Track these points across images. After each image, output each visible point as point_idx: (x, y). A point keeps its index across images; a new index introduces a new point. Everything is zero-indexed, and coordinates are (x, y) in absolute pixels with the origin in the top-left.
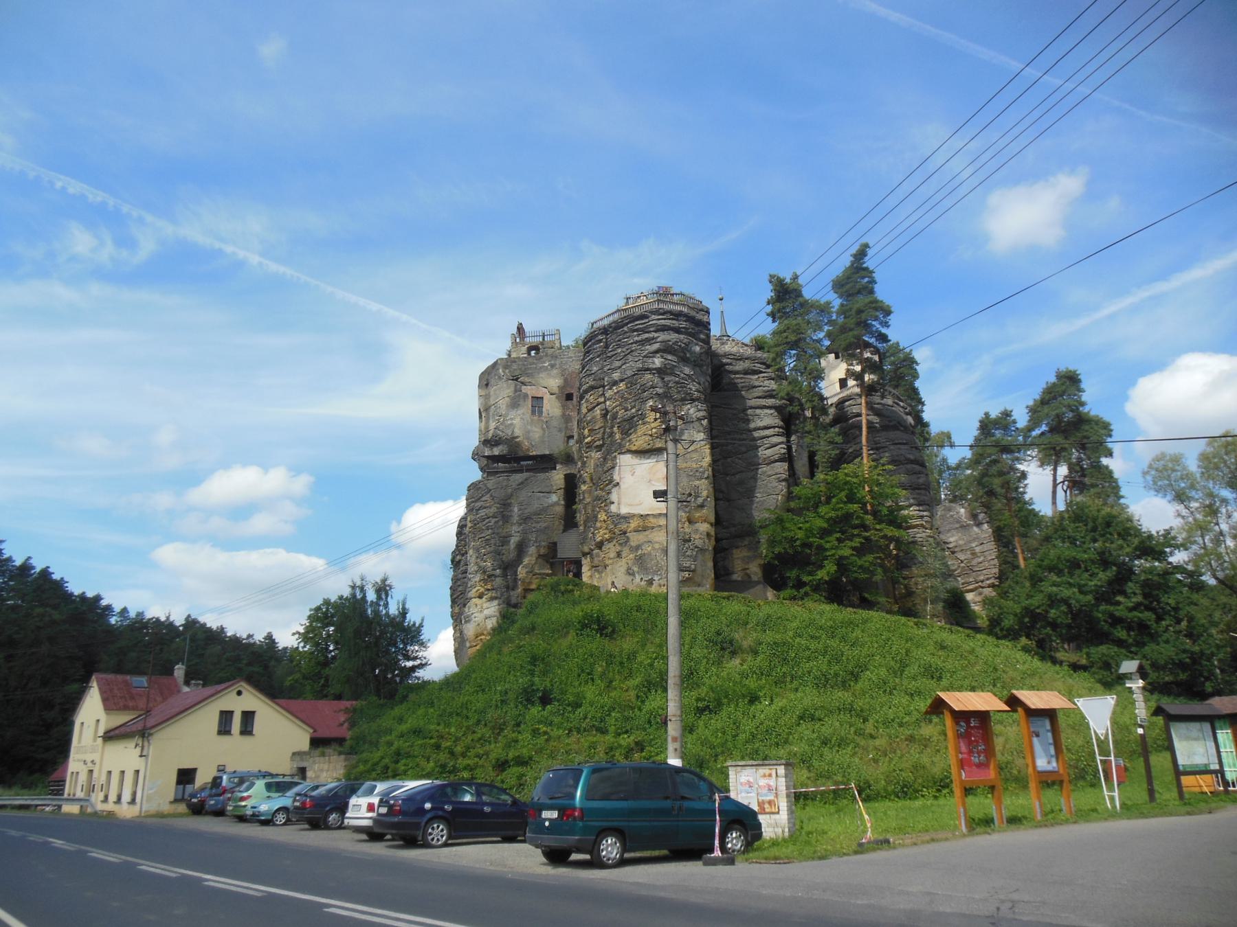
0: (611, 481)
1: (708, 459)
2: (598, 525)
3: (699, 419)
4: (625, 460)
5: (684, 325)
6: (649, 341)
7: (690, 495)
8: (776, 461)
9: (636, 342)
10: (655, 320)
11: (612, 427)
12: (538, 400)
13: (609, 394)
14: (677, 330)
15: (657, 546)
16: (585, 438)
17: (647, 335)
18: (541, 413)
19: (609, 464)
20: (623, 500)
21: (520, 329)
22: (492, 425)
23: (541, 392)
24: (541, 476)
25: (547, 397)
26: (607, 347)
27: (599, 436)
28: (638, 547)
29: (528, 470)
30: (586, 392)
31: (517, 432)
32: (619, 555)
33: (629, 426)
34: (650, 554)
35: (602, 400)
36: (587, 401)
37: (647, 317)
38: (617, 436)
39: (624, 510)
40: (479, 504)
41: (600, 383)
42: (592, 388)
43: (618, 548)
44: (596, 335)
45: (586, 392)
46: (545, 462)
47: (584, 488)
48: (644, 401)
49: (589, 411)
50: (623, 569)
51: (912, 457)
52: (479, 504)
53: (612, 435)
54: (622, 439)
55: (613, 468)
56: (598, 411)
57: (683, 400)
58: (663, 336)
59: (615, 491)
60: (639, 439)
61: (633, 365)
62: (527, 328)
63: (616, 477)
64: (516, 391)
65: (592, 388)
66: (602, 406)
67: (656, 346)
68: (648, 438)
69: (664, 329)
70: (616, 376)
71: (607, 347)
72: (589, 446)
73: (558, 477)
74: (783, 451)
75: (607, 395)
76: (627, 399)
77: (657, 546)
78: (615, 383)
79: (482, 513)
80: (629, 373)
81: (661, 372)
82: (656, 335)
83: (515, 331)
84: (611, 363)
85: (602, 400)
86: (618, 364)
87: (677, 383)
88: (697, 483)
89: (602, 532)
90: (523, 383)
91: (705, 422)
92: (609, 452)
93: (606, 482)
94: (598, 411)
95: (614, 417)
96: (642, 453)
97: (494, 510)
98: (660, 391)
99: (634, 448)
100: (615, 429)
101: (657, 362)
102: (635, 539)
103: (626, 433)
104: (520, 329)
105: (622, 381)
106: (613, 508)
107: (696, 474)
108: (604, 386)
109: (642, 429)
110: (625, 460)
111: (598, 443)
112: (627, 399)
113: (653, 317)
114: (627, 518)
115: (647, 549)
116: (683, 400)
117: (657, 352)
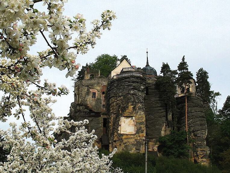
0: (119, 124)
1: (144, 120)
2: (115, 136)
4: (123, 119)
8: (163, 117)
12: (94, 94)
13: (118, 99)
14: (138, 83)
17: (129, 84)
18: (95, 97)
23: (95, 91)
25: (97, 92)
28: (125, 143)
29: (93, 117)
32: (120, 145)
33: (124, 109)
37: (130, 78)
39: (122, 133)
42: (113, 97)
43: (120, 143)
44: (115, 81)
45: (112, 97)
47: (110, 124)
48: (128, 103)
49: (112, 103)
50: (122, 149)
51: (201, 115)
53: (119, 111)
54: (122, 113)
58: (134, 85)
60: (126, 113)
61: (126, 92)
63: (120, 123)
64: (88, 90)
67: (132, 87)
69: (133, 82)
74: (165, 114)
78: (120, 96)
80: (124, 94)
81: (132, 94)
87: (137, 98)
93: (117, 124)
95: (120, 106)
96: (127, 117)
99: (125, 116)
101: (132, 92)
102: (125, 141)
106: (119, 132)
107: (141, 123)
109: (127, 111)
110: (123, 119)
114: (123, 135)
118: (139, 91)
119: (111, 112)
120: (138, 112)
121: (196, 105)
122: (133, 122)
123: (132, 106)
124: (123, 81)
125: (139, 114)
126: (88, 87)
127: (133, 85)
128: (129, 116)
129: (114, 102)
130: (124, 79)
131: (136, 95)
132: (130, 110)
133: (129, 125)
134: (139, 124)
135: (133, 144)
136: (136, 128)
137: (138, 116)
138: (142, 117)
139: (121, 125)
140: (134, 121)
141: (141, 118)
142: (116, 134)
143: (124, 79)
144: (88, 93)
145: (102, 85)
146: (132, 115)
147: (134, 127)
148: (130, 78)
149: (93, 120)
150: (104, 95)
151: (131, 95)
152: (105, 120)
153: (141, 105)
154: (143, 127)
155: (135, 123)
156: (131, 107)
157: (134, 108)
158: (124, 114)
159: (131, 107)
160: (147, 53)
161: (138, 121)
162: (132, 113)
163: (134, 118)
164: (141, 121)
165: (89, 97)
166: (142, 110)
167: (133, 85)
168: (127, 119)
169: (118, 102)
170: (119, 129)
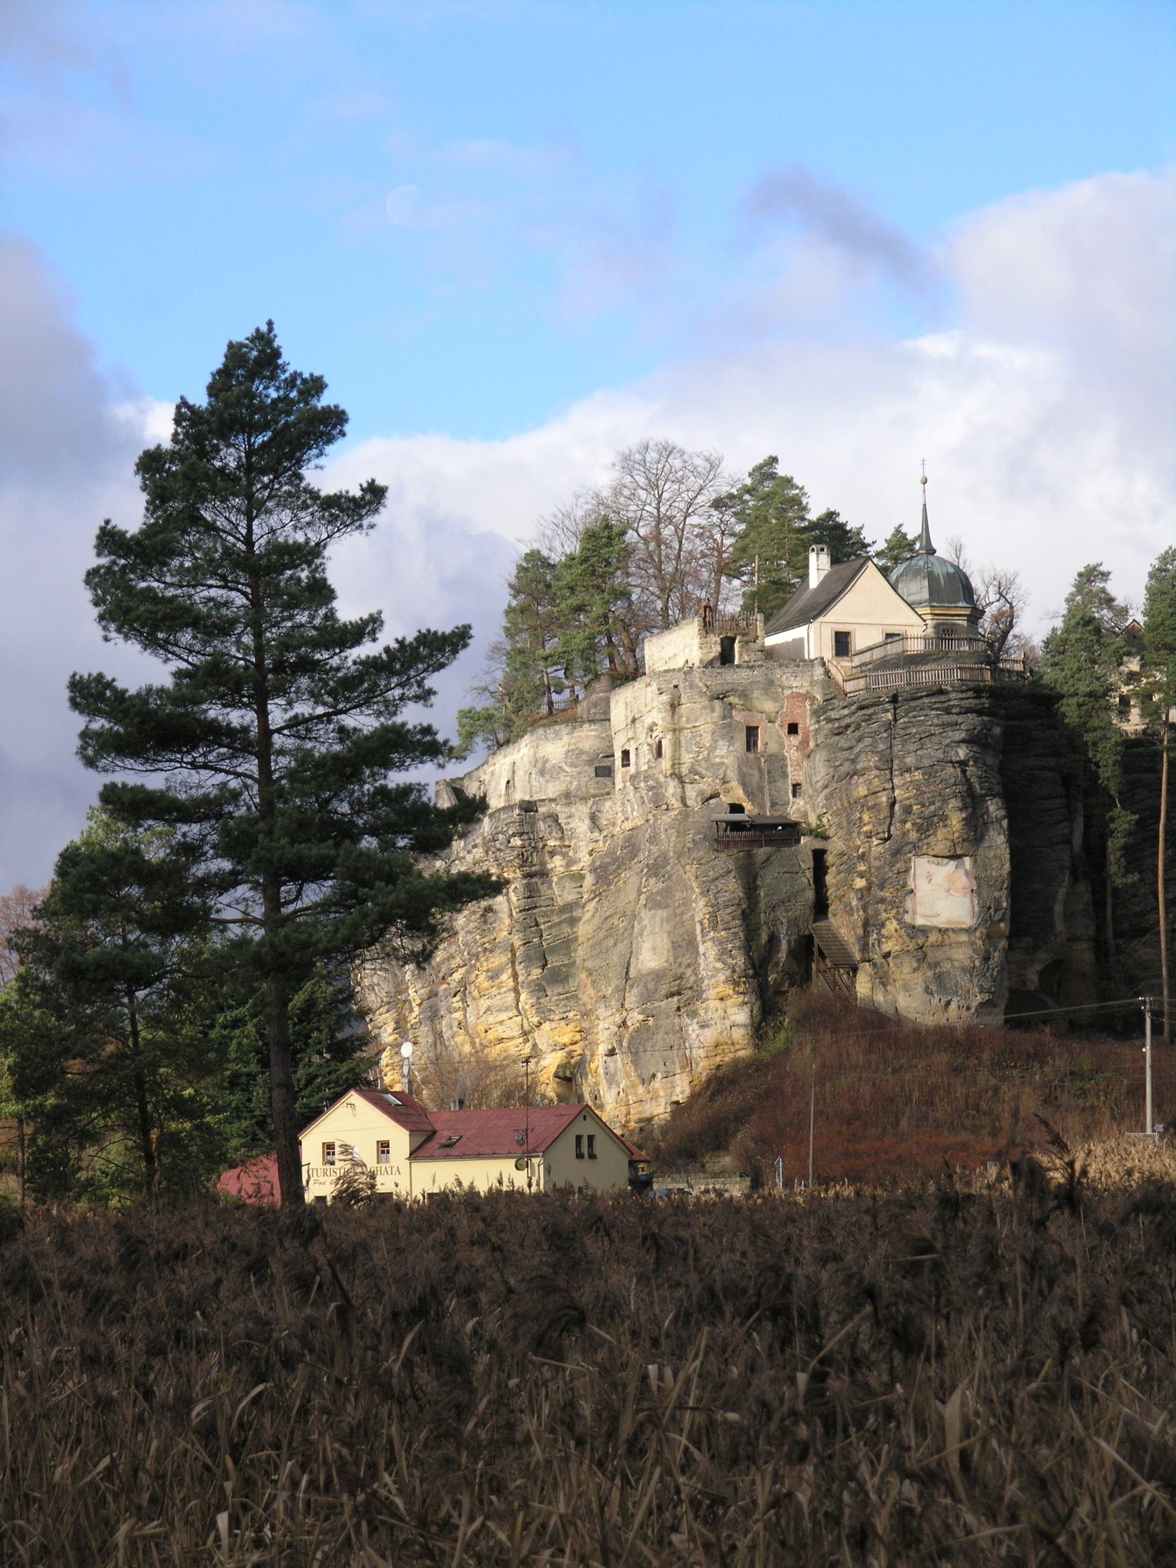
15: (957, 964)
19: (900, 866)
28: (937, 964)
34: (949, 973)
39: (920, 921)
55: (907, 871)
59: (909, 899)
63: (911, 884)
70: (910, 760)
77: (957, 964)
80: (927, 763)
86: (912, 747)
91: (1005, 823)
95: (908, 810)
105: (917, 769)
109: (941, 833)
114: (924, 931)
115: (947, 966)
135: (964, 970)
147: (967, 900)
160: (925, 482)
170: (909, 904)
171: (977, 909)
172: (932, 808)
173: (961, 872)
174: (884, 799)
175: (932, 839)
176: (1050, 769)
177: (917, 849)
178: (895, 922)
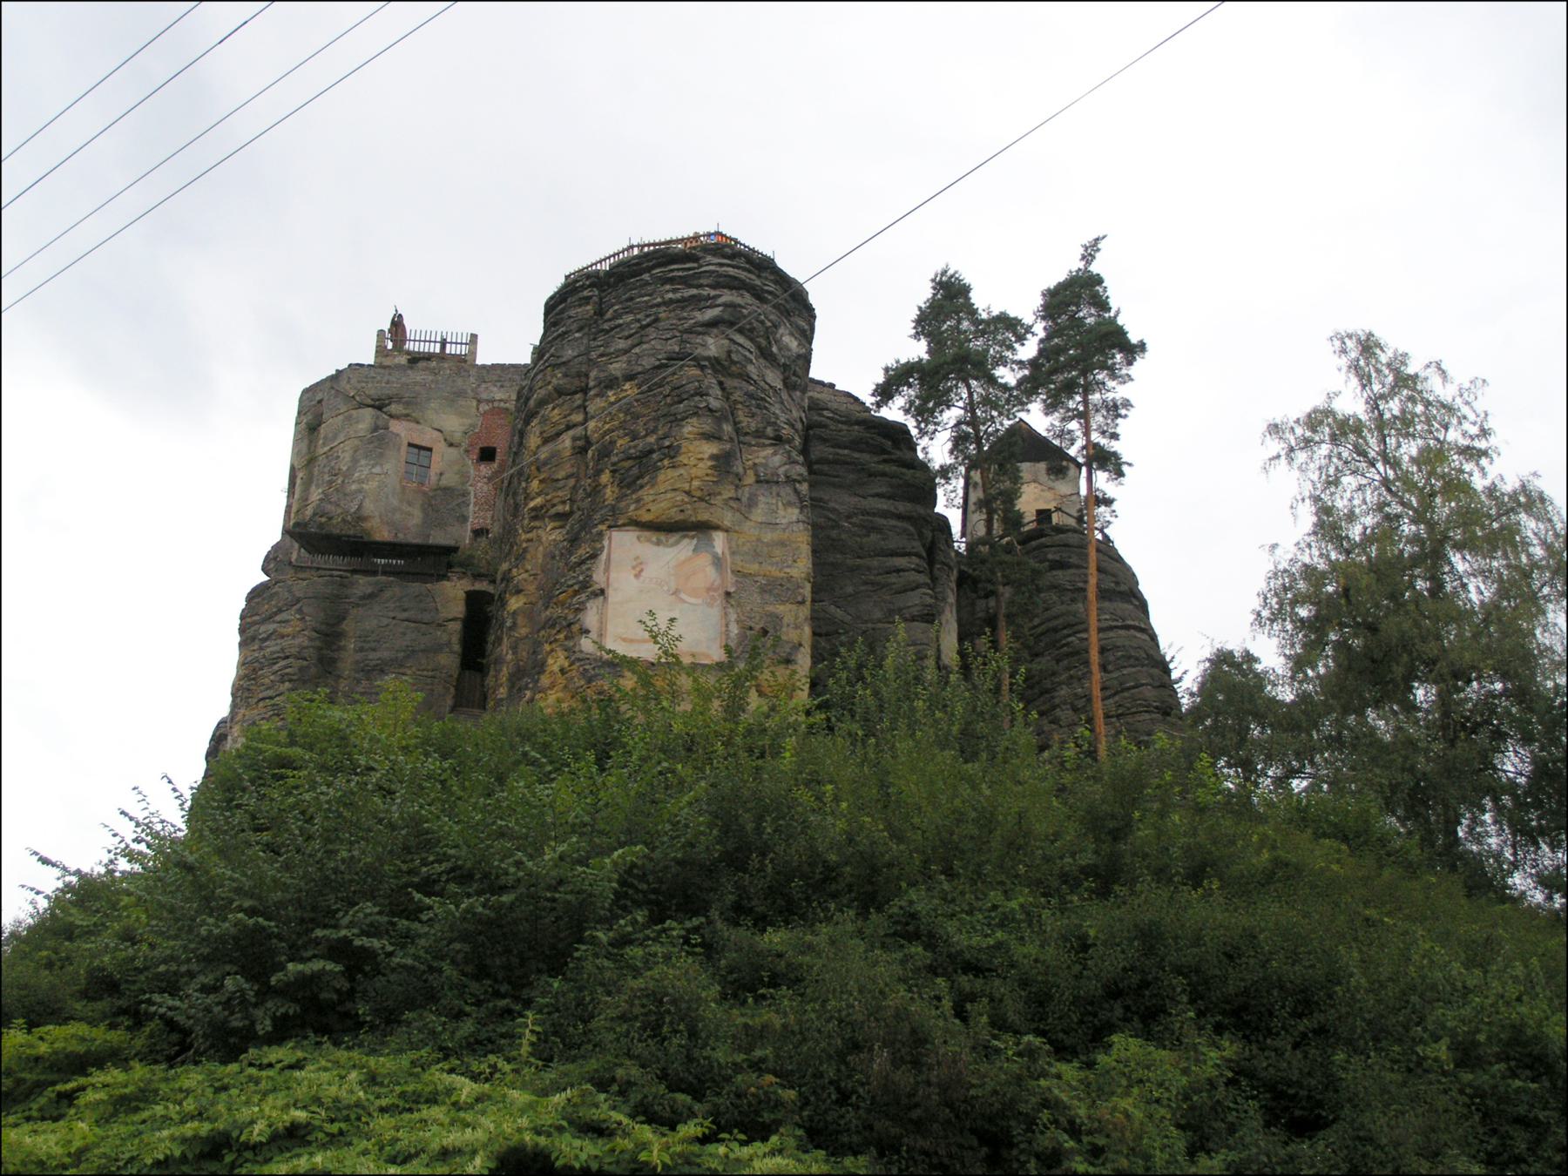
0: (585, 585)
1: (802, 567)
2: (545, 680)
3: (790, 480)
4: (623, 546)
5: (771, 287)
6: (697, 302)
7: (765, 632)
9: (666, 303)
10: (711, 264)
11: (598, 472)
14: (759, 295)
16: (528, 498)
19: (584, 550)
20: (610, 629)
21: (397, 324)
22: (315, 495)
23: (426, 437)
24: (416, 587)
25: (440, 448)
26: (600, 313)
27: (564, 494)
29: (385, 573)
30: (542, 403)
31: (369, 507)
33: (641, 467)
35: (578, 417)
36: (544, 420)
37: (695, 259)
38: (610, 493)
40: (265, 629)
41: (576, 382)
45: (542, 403)
46: (425, 560)
48: (677, 420)
49: (546, 441)
52: (265, 629)
53: (596, 490)
54: (619, 499)
55: (594, 556)
56: (566, 442)
57: (759, 434)
58: (727, 296)
61: (656, 347)
62: (409, 324)
63: (598, 577)
65: (560, 392)
66: (579, 431)
67: (710, 314)
68: (680, 497)
70: (617, 368)
71: (600, 313)
72: (537, 514)
73: (452, 594)
75: (591, 409)
76: (636, 417)
78: (612, 383)
79: (272, 647)
80: (648, 363)
81: (718, 366)
82: (713, 293)
83: (386, 326)
84: (606, 345)
85: (578, 417)
86: (622, 344)
87: (751, 396)
88: (780, 609)
89: (552, 697)
90: (391, 416)
92: (586, 525)
94: (566, 442)
97: (302, 640)
98: (715, 404)
99: (646, 517)
100: (605, 478)
101: (713, 346)
103: (629, 484)
104: (397, 324)
105: (630, 377)
108: (585, 390)
109: (667, 477)
110: (623, 546)
111: (560, 508)
112: (636, 417)
113: (709, 258)
116: (759, 434)
117: (713, 323)
118: (765, 354)
119: (533, 509)
120: (752, 503)
121: (1117, 583)
122: (711, 572)
123: (710, 449)
124: (646, 276)
125: (758, 514)
126: (380, 408)
127: (720, 301)
128: (680, 517)
129: (558, 434)
130: (649, 270)
131: (747, 378)
132: (694, 471)
133: (676, 592)
134: (763, 590)
136: (733, 617)
137: (750, 530)
138: (782, 544)
139: (610, 592)
140: (718, 562)
141: (777, 552)
142: (557, 661)
143: (654, 267)
144: (379, 440)
145: (484, 407)
146: (704, 516)
147: (715, 613)
148: (695, 259)
149: (387, 594)
150: (486, 470)
151: (702, 368)
152: (473, 599)
153: (777, 460)
154: (796, 625)
155: (730, 577)
156: (698, 454)
157: (723, 463)
158: (638, 501)
159: (698, 454)
161: (753, 568)
162: (705, 498)
163: (719, 540)
164: (775, 572)
165: (377, 470)
166: (789, 490)
167: (720, 301)
168: (658, 543)
169: (592, 424)
170: (590, 618)
171: (735, 630)
172: (652, 439)
173: (704, 560)
174: (568, 443)
175: (647, 494)
176: (899, 517)
177: (617, 520)
178: (561, 655)
